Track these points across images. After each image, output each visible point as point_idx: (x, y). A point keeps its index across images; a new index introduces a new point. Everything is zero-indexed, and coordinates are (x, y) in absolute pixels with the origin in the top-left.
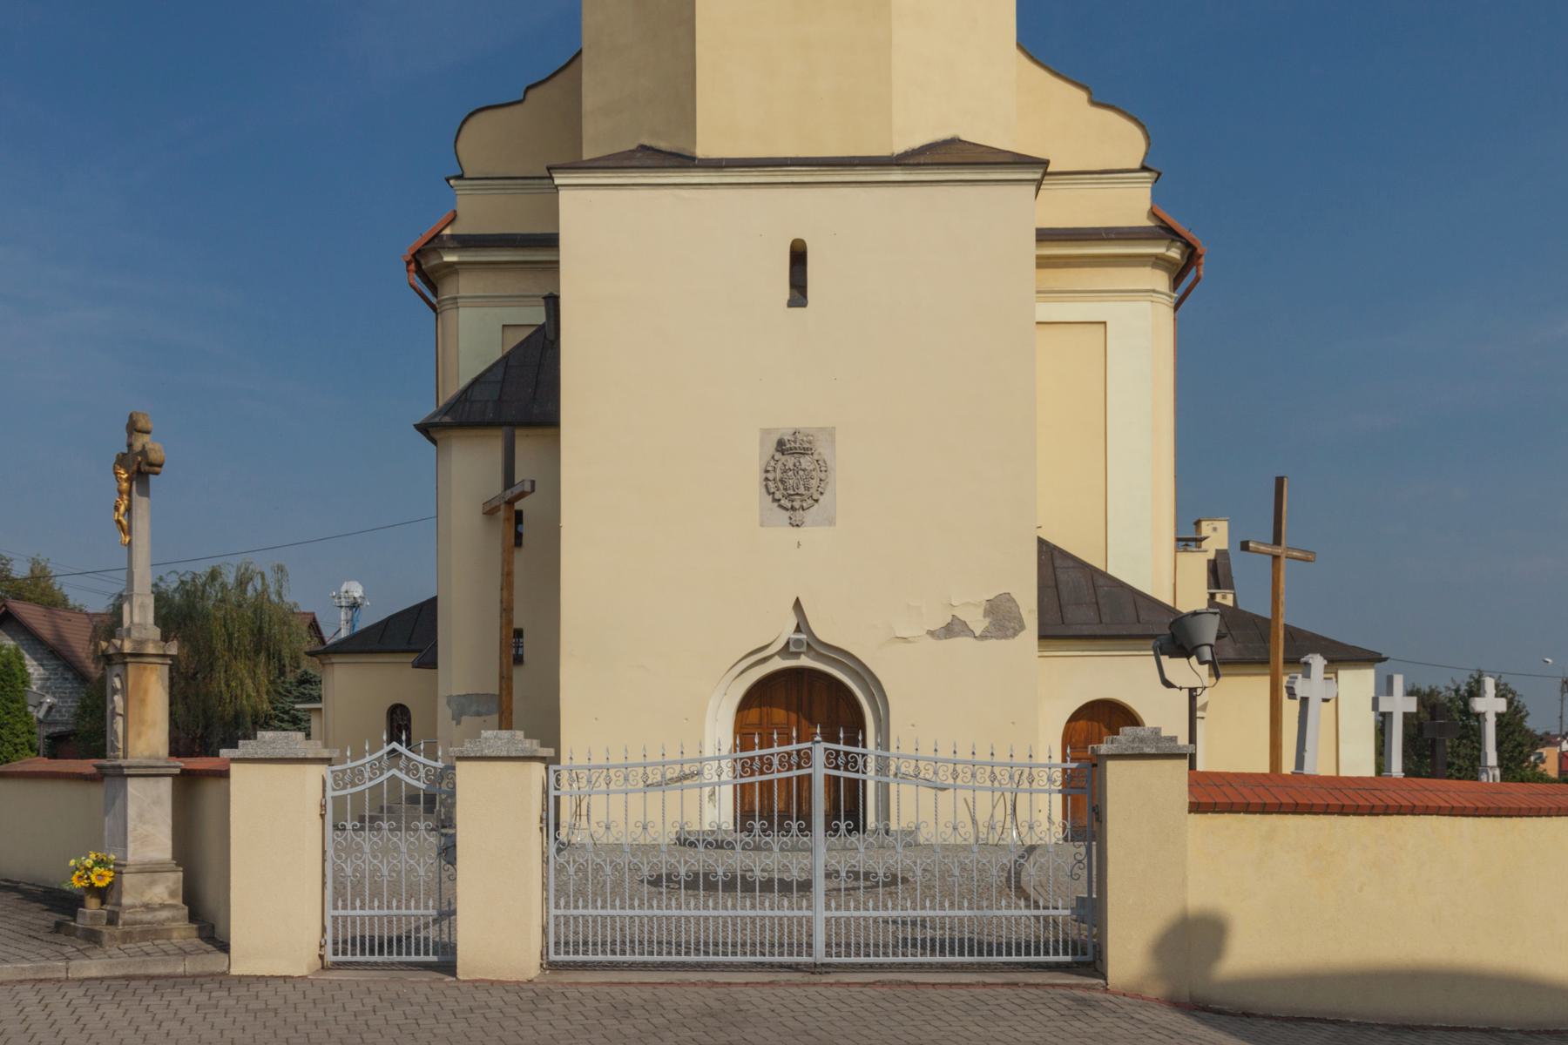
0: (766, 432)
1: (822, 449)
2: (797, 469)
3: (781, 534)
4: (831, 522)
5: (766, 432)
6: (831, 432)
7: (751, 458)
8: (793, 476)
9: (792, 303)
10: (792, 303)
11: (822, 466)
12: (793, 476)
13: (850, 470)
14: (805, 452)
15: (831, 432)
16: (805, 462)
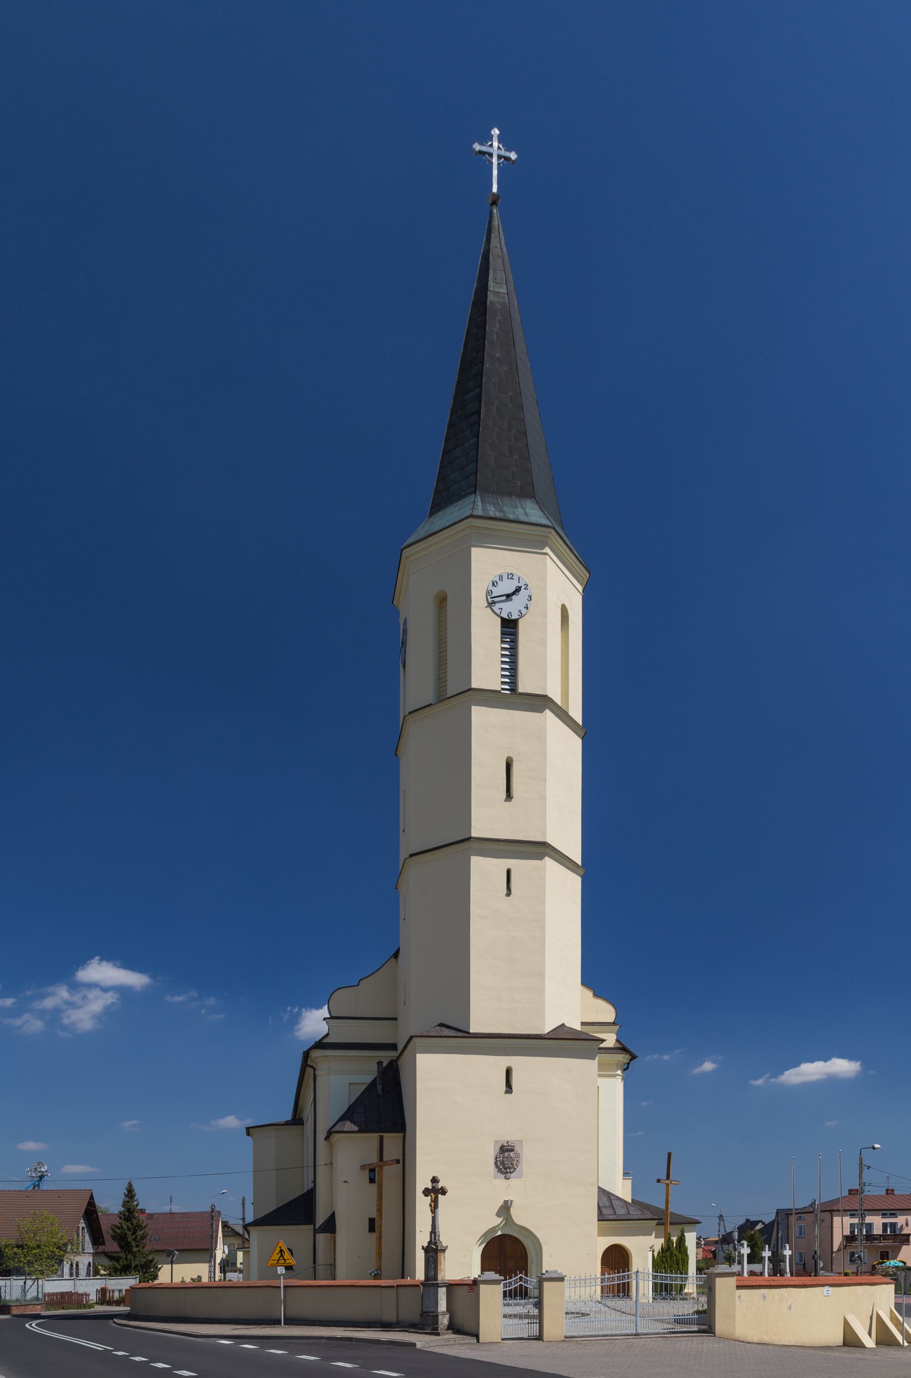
0: (496, 1142)
1: (516, 1148)
2: (509, 1157)
3: (501, 1181)
4: (520, 1177)
5: (496, 1142)
6: (521, 1142)
7: (490, 1153)
8: (506, 1160)
9: (507, 1092)
10: (507, 1092)
11: (518, 1155)
12: (506, 1160)
13: (528, 1156)
14: (512, 1150)
15: (521, 1142)
16: (511, 1154)
